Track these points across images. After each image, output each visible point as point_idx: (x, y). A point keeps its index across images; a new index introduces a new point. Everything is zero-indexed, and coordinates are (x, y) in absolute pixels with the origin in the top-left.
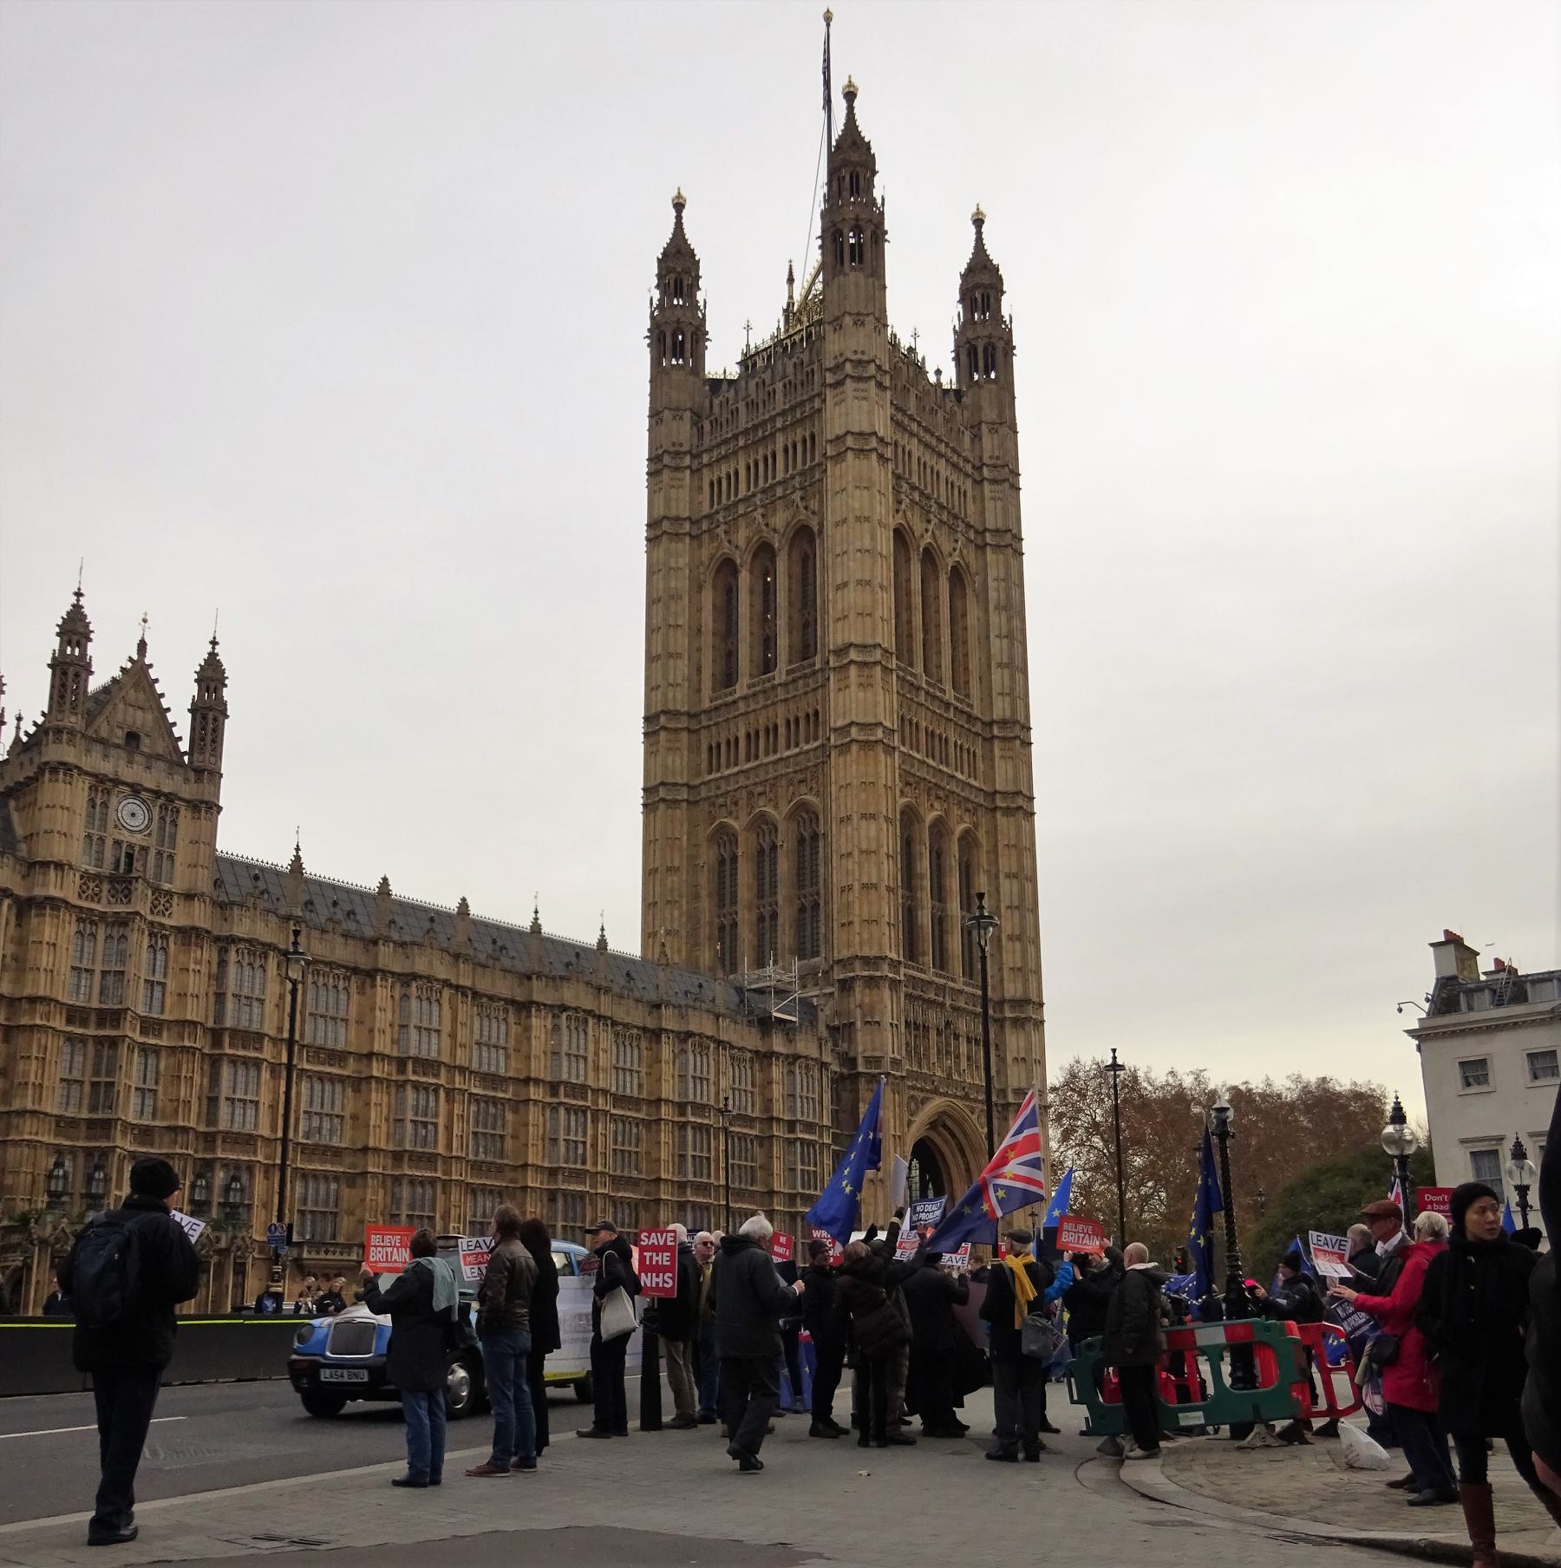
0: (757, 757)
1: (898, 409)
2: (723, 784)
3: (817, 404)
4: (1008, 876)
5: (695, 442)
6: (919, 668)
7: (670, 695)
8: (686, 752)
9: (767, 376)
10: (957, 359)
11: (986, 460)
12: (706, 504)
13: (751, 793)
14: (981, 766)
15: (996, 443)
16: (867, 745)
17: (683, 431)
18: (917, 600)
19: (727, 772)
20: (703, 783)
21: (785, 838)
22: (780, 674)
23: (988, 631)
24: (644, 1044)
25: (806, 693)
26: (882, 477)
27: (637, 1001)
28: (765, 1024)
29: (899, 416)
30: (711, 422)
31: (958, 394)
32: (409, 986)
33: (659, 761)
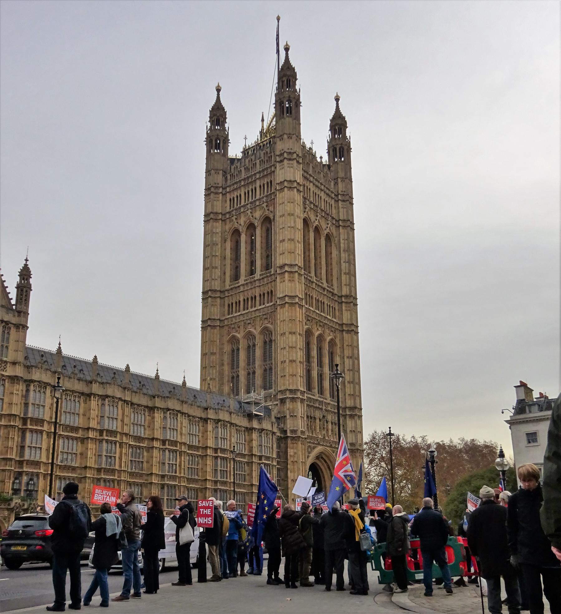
0: (248, 309)
1: (305, 171)
2: (234, 319)
3: (273, 169)
4: (348, 357)
5: (224, 183)
6: (313, 274)
7: (213, 283)
8: (219, 307)
9: (253, 157)
10: (329, 152)
11: (340, 192)
12: (228, 207)
13: (245, 323)
14: (337, 314)
15: (344, 186)
16: (292, 304)
17: (219, 179)
18: (312, 247)
20: (226, 319)
21: (259, 342)
22: (257, 276)
24: (201, 424)
25: (267, 283)
26: (298, 198)
28: (250, 416)
29: (306, 174)
31: (329, 166)
32: (105, 400)
33: (208, 310)
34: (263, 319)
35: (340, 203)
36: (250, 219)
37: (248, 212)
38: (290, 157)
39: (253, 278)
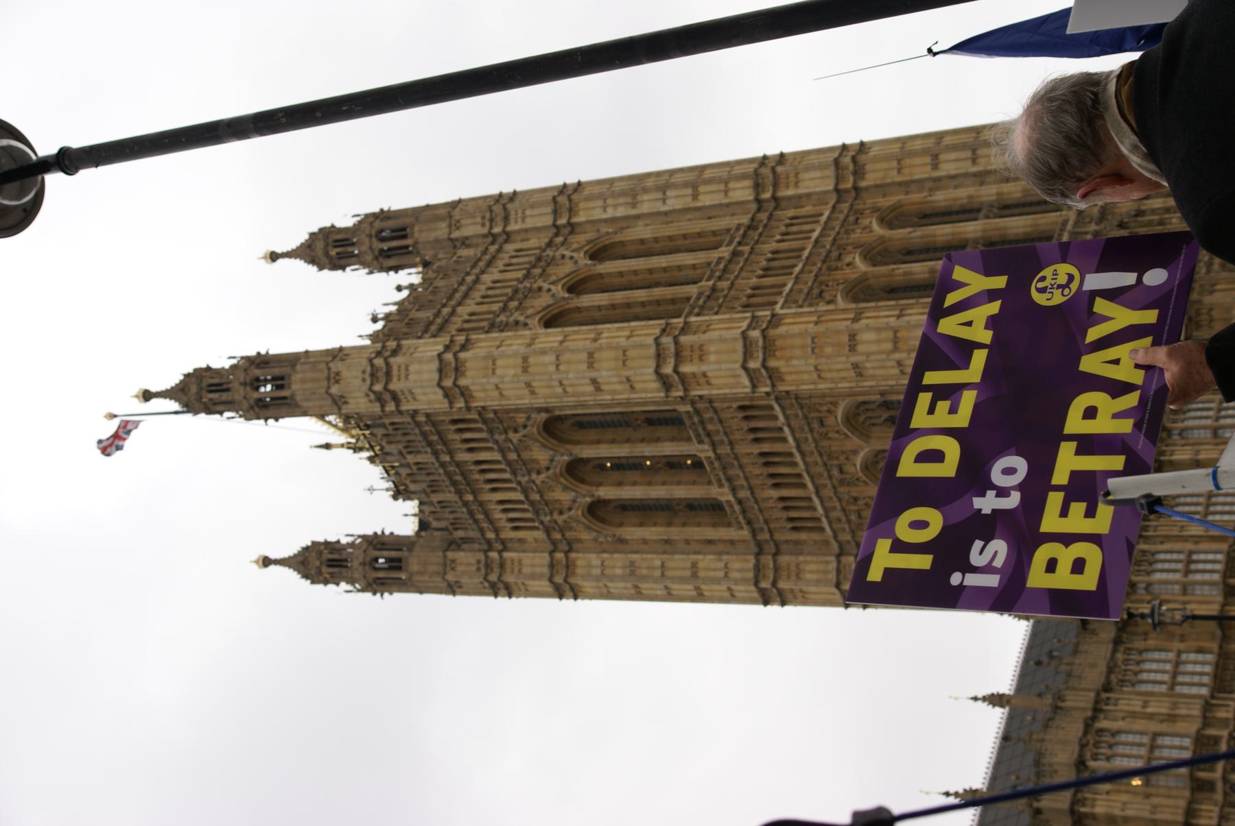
0: (799, 475)
1: (426, 331)
3: (422, 419)
4: (935, 166)
5: (476, 546)
6: (693, 290)
7: (737, 575)
8: (801, 558)
11: (485, 231)
13: (842, 482)
14: (808, 209)
15: (470, 221)
16: (769, 348)
17: (466, 559)
18: (619, 297)
19: (820, 510)
20: (835, 537)
22: (704, 451)
23: (658, 214)
24: (1139, 644)
25: (721, 421)
26: (484, 344)
27: (1075, 652)
29: (433, 328)
30: (457, 529)
31: (426, 264)
33: (813, 589)
34: (823, 430)
35: (512, 227)
36: (555, 477)
37: (538, 482)
38: (381, 374)
39: (711, 463)
